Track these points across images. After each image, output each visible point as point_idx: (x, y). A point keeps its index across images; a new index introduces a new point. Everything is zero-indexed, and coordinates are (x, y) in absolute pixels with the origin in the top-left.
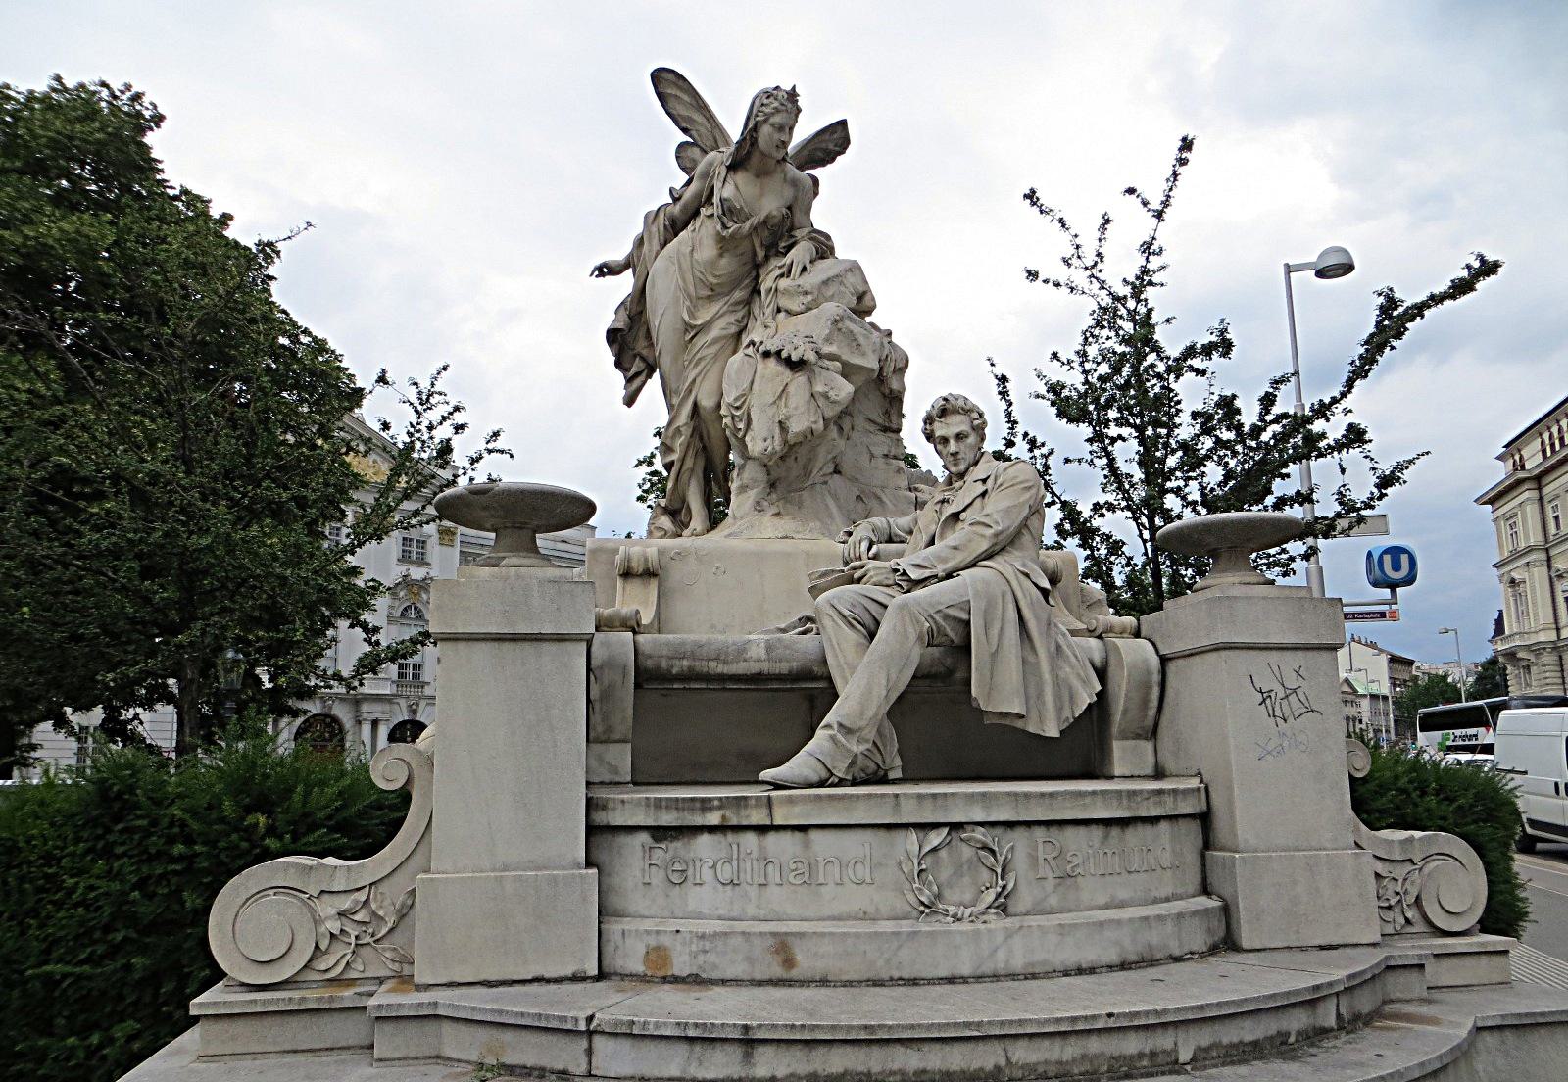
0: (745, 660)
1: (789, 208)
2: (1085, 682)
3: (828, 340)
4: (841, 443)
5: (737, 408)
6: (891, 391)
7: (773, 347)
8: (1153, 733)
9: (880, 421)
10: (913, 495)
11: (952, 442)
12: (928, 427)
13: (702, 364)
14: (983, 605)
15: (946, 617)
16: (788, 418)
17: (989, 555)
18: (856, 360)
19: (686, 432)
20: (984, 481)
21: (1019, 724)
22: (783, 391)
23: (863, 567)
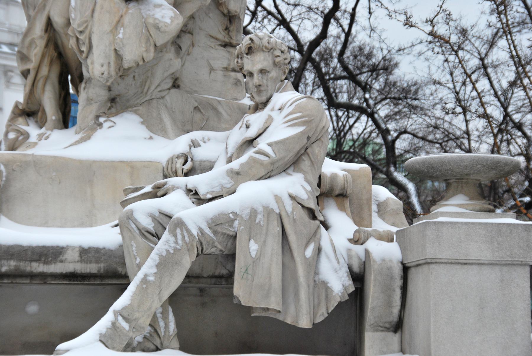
0: (61, 261)
4: (177, 63)
5: (81, 32)
6: (229, 12)
8: (398, 326)
12: (239, 60)
19: (41, 44)
21: (281, 318)
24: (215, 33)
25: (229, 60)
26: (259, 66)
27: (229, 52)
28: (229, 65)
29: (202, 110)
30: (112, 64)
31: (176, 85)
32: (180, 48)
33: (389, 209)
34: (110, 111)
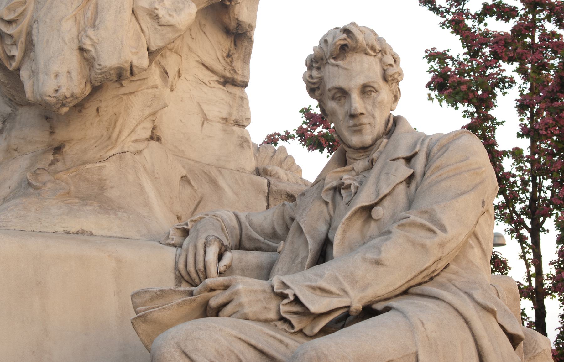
9: (218, 67)
10: (263, 181)
12: (315, 73)
20: (408, 160)
23: (226, 287)
24: (209, 61)
25: (231, 107)
26: (360, 80)
27: (230, 93)
28: (230, 114)
29: (193, 183)
30: (74, 74)
31: (155, 136)
32: (167, 73)
33: (540, 351)
34: (53, 167)
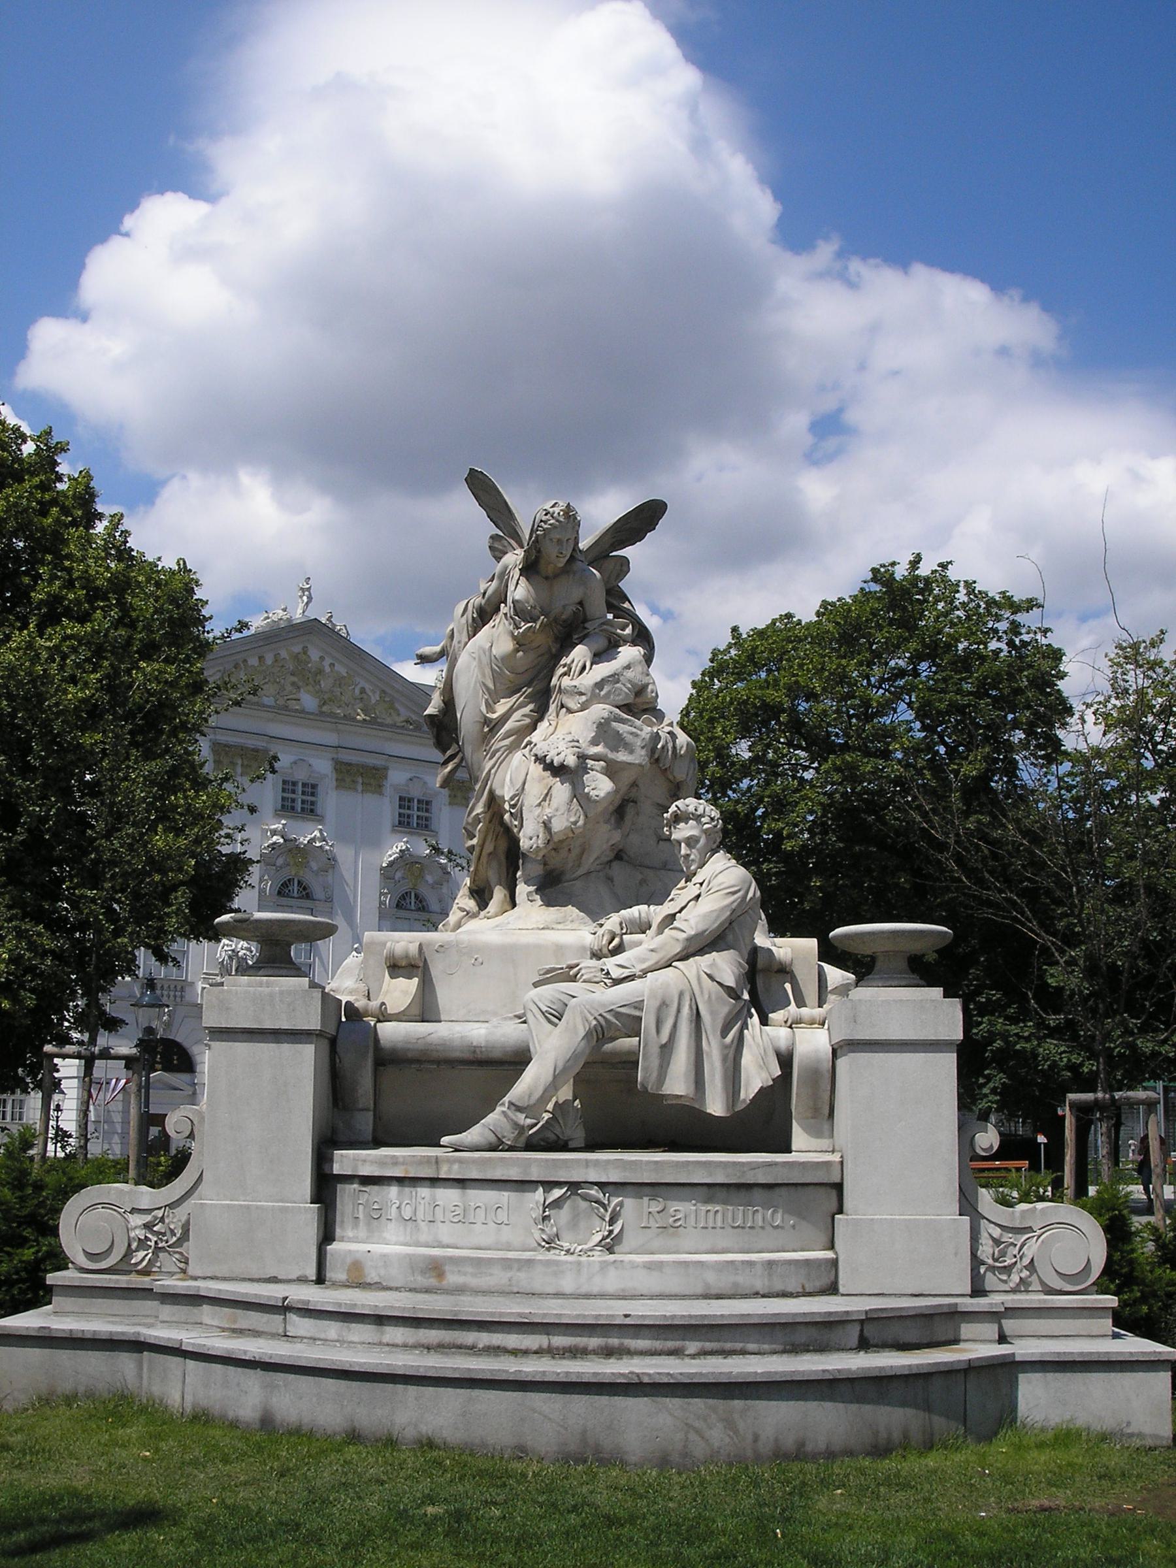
1: (581, 603)
2: (764, 1065)
3: (594, 742)
5: (513, 806)
7: (540, 750)
11: (683, 845)
13: (497, 755)
14: (657, 1003)
15: (617, 1015)
16: (550, 819)
17: (684, 957)
18: (622, 756)
20: (701, 884)
22: (547, 795)
